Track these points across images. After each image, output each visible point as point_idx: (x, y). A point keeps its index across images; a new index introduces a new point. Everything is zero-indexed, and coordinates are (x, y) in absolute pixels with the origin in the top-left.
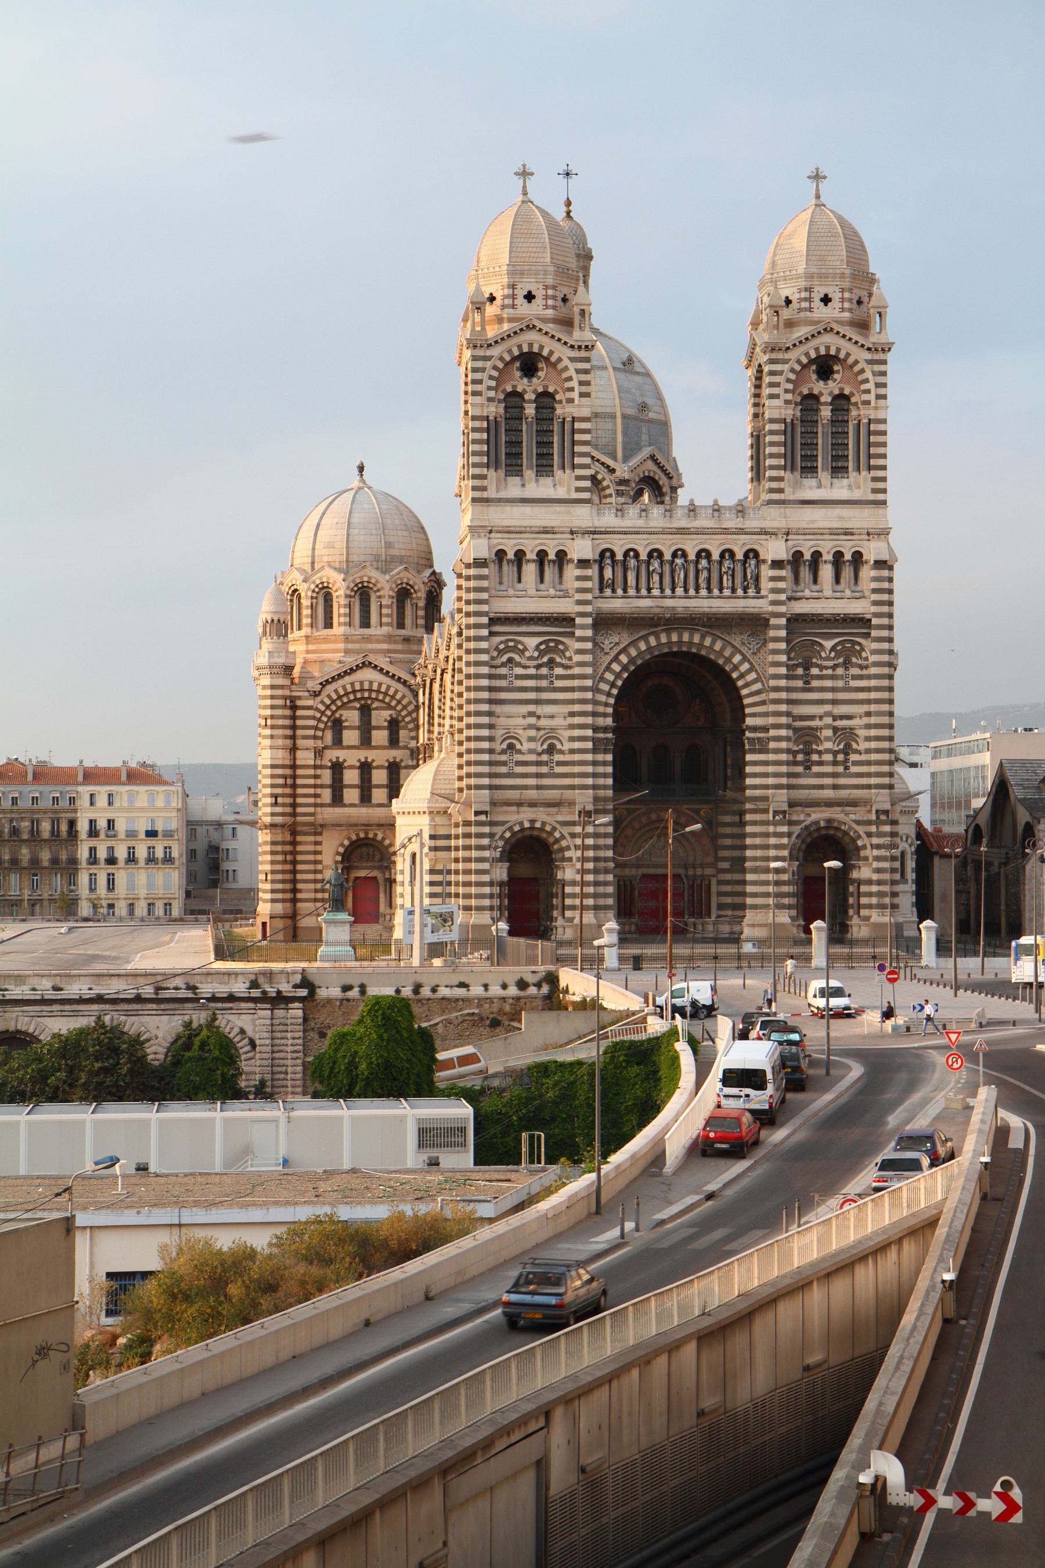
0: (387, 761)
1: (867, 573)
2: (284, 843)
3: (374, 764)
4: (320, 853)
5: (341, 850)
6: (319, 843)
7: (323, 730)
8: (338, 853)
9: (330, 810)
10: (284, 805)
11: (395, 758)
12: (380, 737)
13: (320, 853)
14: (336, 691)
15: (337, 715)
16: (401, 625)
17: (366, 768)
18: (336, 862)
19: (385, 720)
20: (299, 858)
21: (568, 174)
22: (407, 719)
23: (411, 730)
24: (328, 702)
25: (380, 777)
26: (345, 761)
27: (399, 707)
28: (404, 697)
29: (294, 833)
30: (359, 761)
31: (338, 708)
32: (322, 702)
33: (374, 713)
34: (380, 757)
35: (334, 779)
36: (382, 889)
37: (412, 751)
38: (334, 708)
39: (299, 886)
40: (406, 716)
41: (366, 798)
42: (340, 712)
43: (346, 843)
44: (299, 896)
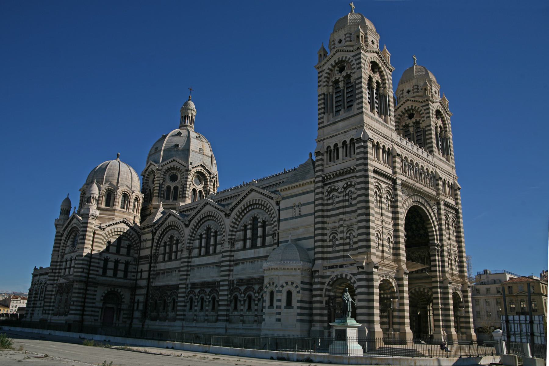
0: (125, 261)
2: (83, 289)
3: (120, 261)
4: (95, 295)
5: (104, 295)
6: (96, 291)
7: (103, 244)
8: (102, 296)
9: (101, 278)
10: (86, 273)
11: (128, 260)
12: (123, 251)
13: (95, 295)
14: (111, 230)
15: (109, 240)
16: (133, 211)
17: (117, 262)
18: (101, 300)
19: (127, 245)
20: (87, 296)
21: (190, 90)
22: (135, 246)
23: (135, 250)
24: (107, 234)
25: (121, 267)
26: (109, 258)
27: (133, 241)
28: (135, 237)
29: (87, 286)
30: (115, 259)
31: (111, 237)
32: (105, 233)
33: (123, 241)
34: (123, 259)
35: (104, 266)
36: (115, 312)
37: (135, 259)
38: (109, 236)
39: (85, 309)
40: (135, 244)
41: (115, 275)
42: (110, 239)
43: (106, 292)
44: (85, 313)
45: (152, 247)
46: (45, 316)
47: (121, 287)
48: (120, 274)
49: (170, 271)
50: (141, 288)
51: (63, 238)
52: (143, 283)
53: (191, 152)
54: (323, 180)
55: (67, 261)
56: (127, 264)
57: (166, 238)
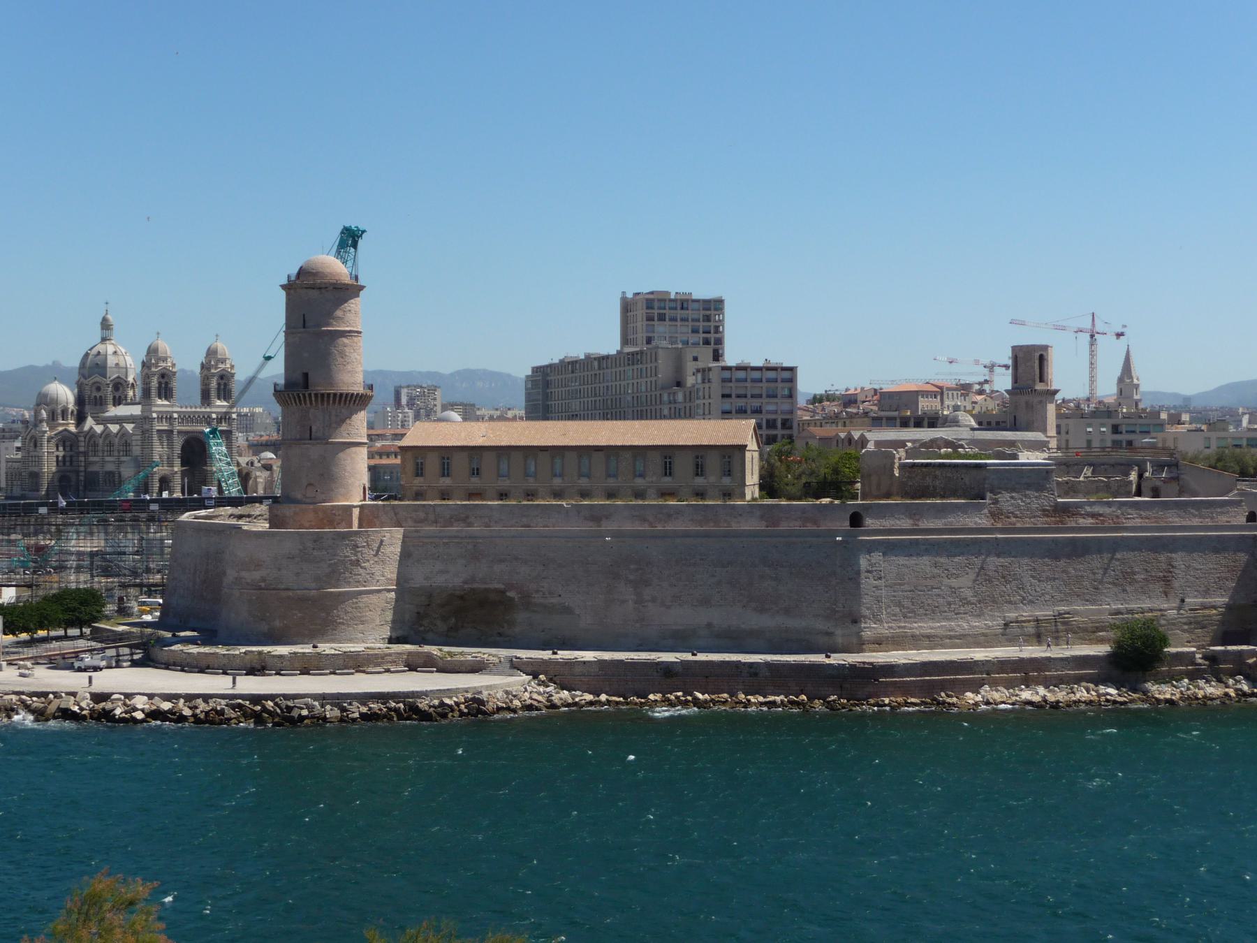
1: (230, 421)
12: (68, 449)
21: (107, 303)
25: (68, 459)
34: (69, 454)
41: (64, 464)
45: (85, 446)
46: (24, 492)
47: (70, 472)
48: (68, 464)
49: (96, 462)
50: (81, 471)
51: (27, 441)
52: (82, 469)
53: (108, 369)
54: (142, 432)
55: (32, 457)
56: (71, 457)
57: (92, 442)
